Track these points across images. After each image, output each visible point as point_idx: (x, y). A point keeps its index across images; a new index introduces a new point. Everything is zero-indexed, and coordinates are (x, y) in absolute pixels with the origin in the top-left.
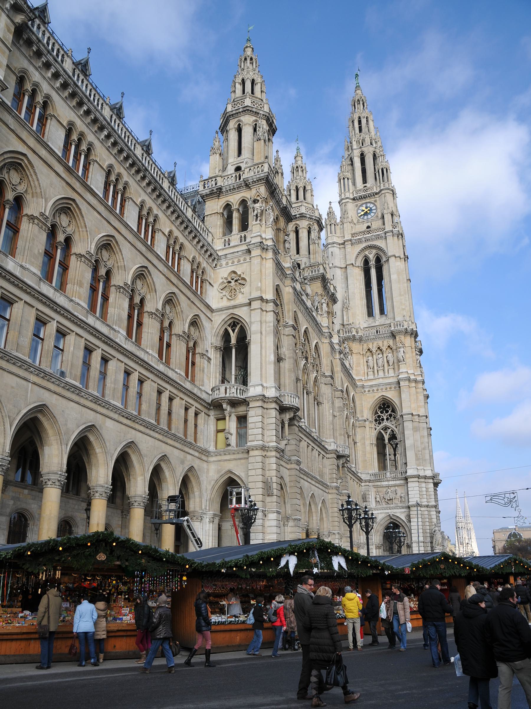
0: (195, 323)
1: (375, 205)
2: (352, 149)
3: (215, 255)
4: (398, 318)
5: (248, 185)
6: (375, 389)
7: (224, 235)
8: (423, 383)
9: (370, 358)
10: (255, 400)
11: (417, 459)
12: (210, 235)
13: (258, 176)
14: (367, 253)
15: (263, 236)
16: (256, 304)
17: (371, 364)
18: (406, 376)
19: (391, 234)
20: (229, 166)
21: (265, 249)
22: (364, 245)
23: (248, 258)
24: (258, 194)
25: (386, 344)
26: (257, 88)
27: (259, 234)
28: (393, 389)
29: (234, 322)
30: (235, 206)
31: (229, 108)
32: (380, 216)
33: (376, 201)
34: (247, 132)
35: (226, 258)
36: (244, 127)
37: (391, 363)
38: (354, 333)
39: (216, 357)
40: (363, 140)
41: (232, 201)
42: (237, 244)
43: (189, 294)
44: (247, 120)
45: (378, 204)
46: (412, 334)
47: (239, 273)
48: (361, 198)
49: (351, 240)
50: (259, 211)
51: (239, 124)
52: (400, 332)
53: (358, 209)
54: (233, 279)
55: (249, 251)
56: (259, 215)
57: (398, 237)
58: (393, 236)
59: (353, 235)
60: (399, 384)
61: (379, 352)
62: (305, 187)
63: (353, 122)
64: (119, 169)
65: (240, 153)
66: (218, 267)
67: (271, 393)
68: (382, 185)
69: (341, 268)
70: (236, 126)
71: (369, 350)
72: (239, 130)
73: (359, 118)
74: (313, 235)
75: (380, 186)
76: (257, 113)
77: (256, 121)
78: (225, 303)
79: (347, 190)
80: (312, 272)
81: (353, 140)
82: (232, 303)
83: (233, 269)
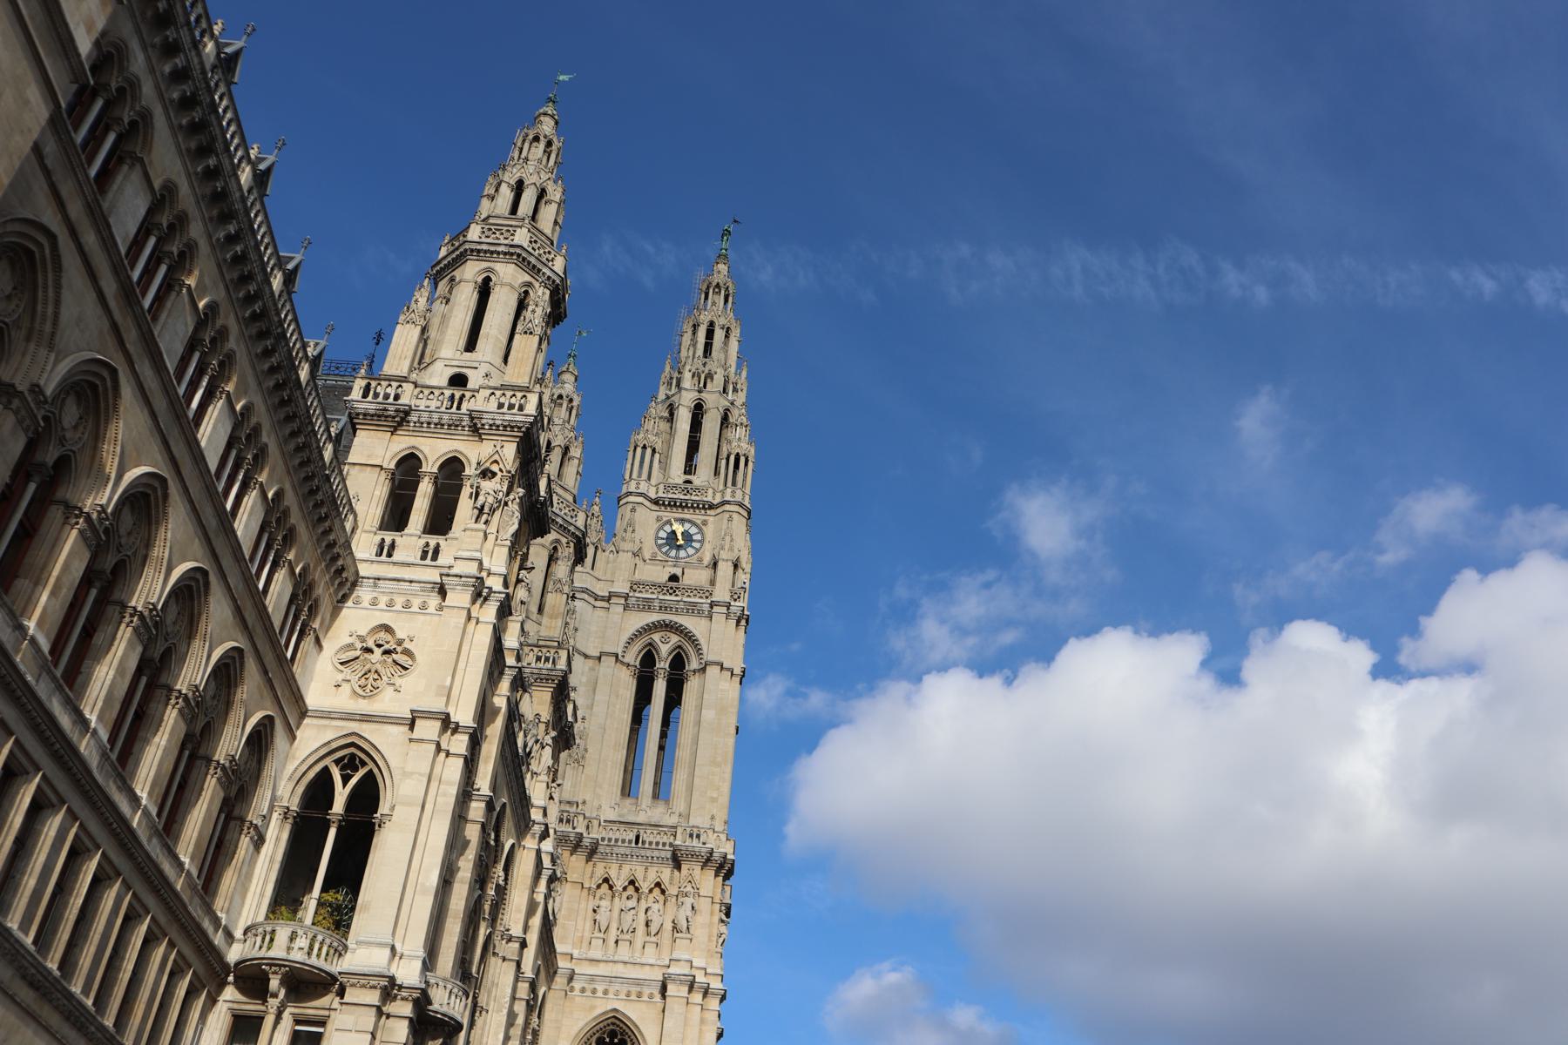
0: (260, 742)
1: (701, 531)
2: (678, 385)
3: (352, 570)
5: (476, 430)
6: (600, 988)
7: (384, 526)
8: (723, 998)
9: (605, 903)
10: (363, 986)
12: (351, 517)
13: (508, 417)
14: (656, 637)
15: (486, 564)
17: (602, 917)
18: (687, 971)
19: (724, 610)
20: (438, 365)
21: (480, 593)
22: (654, 617)
23: (434, 600)
24: (496, 457)
25: (652, 877)
26: (548, 214)
27: (477, 555)
28: (645, 998)
29: (353, 756)
30: (430, 466)
31: (474, 233)
32: (707, 559)
33: (705, 523)
35: (375, 585)
36: (497, 289)
37: (653, 929)
38: (581, 829)
39: (277, 837)
40: (710, 376)
41: (426, 451)
42: (411, 560)
43: (269, 658)
44: (508, 275)
45: (709, 531)
46: (721, 866)
47: (400, 634)
48: (673, 504)
49: (627, 597)
50: (490, 500)
51: (487, 280)
52: (693, 855)
53: (661, 528)
54: (379, 646)
55: (442, 592)
56: (486, 510)
57: (738, 622)
58: (728, 616)
59: (635, 585)
60: (664, 989)
61: (631, 890)
62: (567, 449)
63: (695, 327)
64: (229, 320)
65: (471, 345)
66: (350, 603)
67: (409, 973)
68: (729, 490)
69: (586, 656)
70: (480, 280)
71: (606, 880)
72: (485, 290)
73: (712, 324)
74: (561, 569)
75: (723, 492)
76: (534, 270)
77: (529, 285)
78: (344, 701)
79: (645, 476)
80: (538, 659)
81: (688, 367)
82: (363, 706)
83: (386, 618)
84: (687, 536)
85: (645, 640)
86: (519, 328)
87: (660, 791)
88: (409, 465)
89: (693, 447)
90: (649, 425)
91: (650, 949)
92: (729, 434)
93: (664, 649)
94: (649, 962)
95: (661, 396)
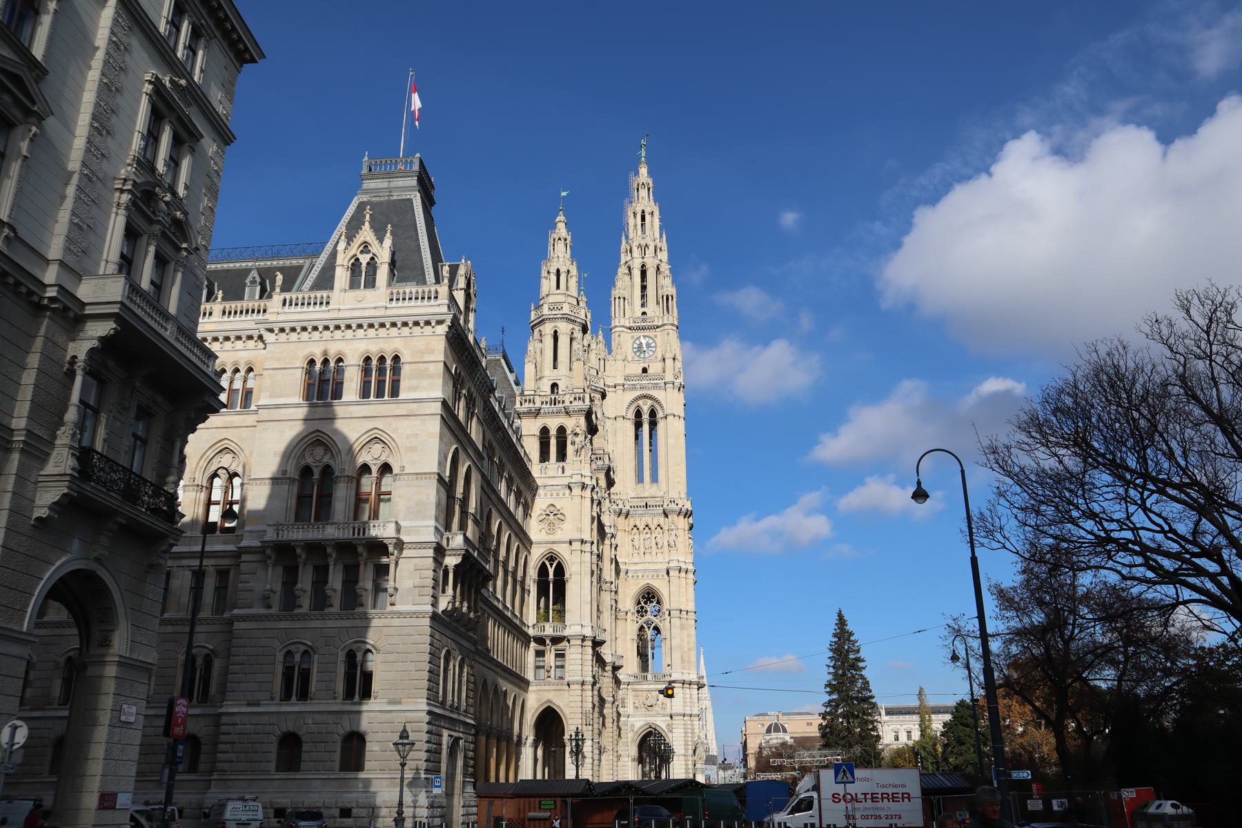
4: (673, 495)
11: (683, 661)
14: (640, 402)
16: (576, 545)
17: (636, 543)
21: (584, 487)
22: (638, 393)
30: (553, 432)
32: (660, 357)
34: (563, 342)
38: (621, 506)
44: (564, 328)
45: (658, 340)
48: (639, 329)
51: (556, 332)
59: (627, 378)
67: (588, 632)
84: (648, 345)
85: (635, 405)
86: (574, 359)
87: (655, 479)
88: (545, 431)
89: (644, 288)
90: (619, 284)
91: (659, 555)
92: (661, 277)
93: (645, 407)
94: (660, 561)
95: (623, 261)
